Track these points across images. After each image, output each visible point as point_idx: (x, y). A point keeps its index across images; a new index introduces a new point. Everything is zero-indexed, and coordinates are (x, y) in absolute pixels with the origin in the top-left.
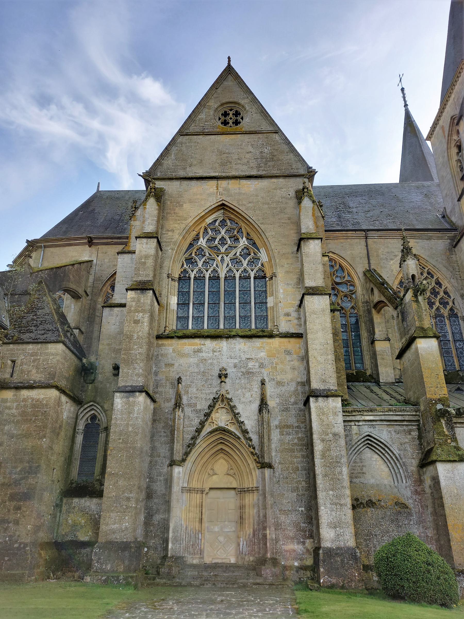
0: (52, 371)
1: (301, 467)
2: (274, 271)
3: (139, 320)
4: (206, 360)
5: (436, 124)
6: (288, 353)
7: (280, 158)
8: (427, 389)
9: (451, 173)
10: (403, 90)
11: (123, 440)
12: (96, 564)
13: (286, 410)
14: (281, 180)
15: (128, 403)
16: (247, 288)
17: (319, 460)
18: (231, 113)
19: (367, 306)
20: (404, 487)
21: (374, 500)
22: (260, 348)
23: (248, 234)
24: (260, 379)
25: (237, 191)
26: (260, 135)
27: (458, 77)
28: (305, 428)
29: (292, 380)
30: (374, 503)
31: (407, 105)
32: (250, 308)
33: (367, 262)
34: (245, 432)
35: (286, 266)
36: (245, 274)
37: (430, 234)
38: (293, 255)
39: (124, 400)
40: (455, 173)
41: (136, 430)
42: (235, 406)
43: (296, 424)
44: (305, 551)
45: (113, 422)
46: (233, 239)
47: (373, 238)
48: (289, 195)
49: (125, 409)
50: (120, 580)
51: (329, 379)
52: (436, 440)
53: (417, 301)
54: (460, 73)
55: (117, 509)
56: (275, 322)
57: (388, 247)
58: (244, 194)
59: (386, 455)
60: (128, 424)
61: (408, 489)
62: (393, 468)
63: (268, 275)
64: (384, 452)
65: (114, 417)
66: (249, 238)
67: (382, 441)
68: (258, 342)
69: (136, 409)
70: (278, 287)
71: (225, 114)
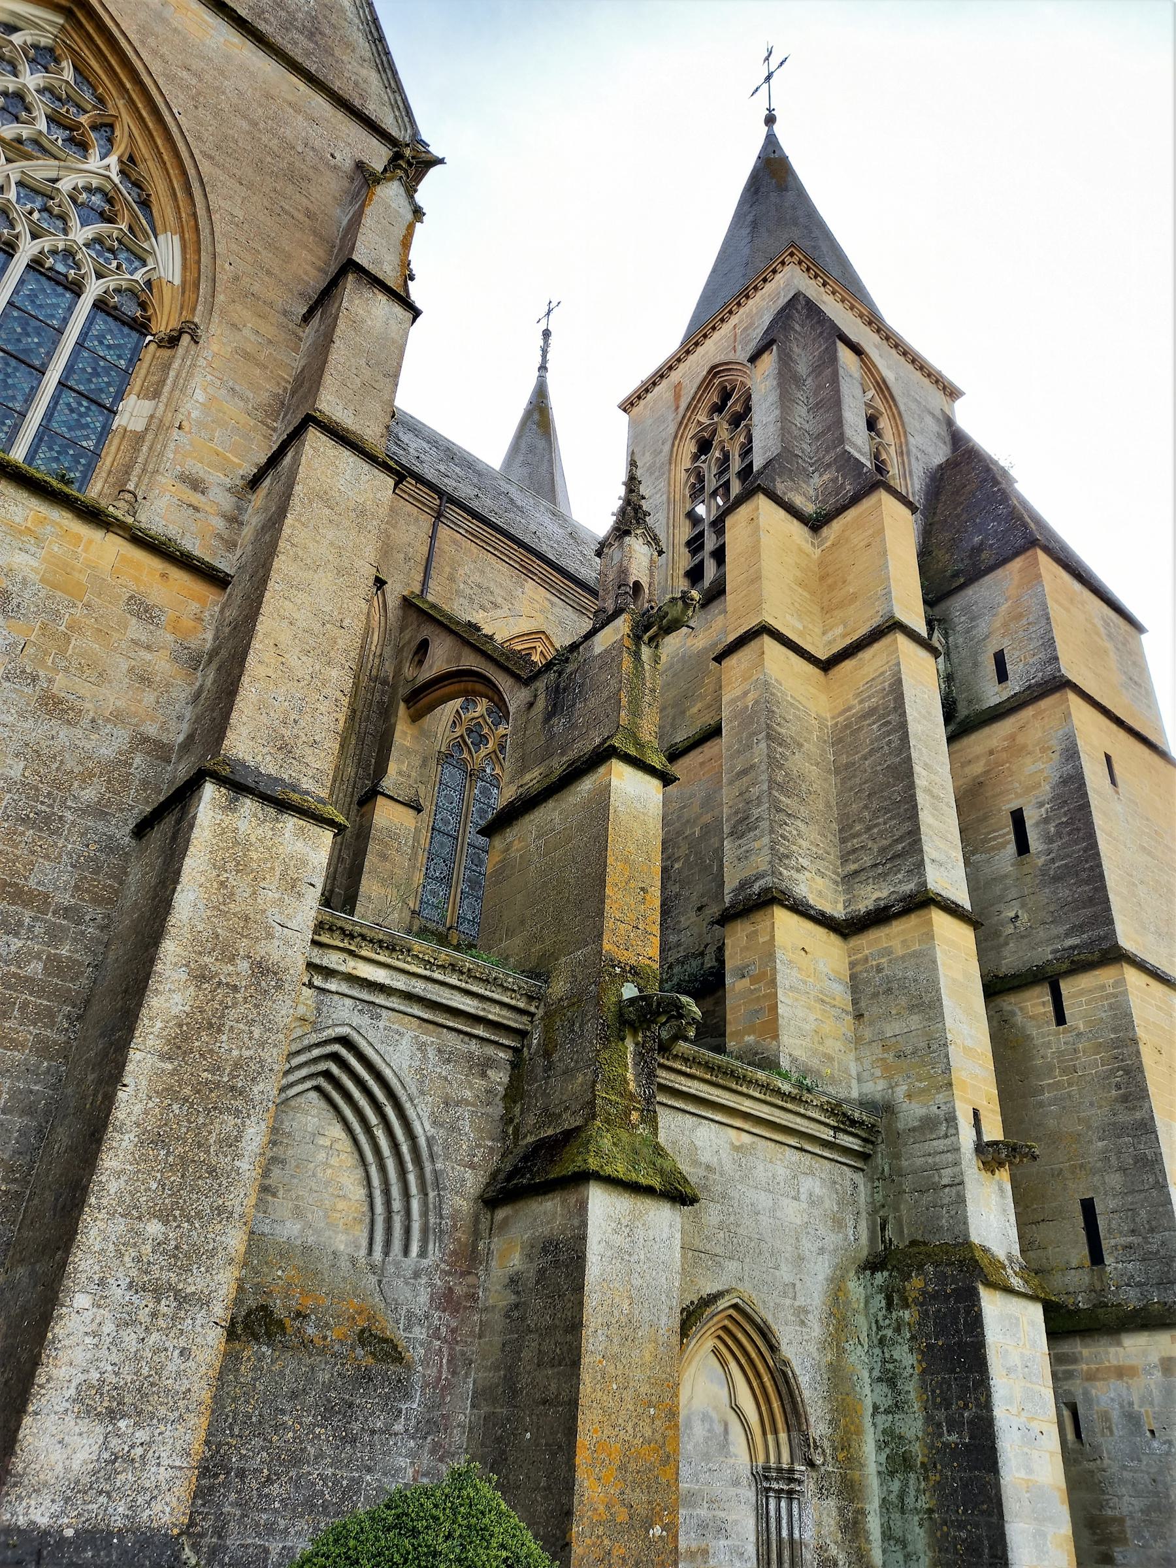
2: (196, 320)
5: (662, 376)
6: (143, 611)
7: (337, 53)
8: (609, 924)
9: (669, 492)
10: (547, 334)
13: (46, 823)
16: (52, 316)
17: (151, 1060)
19: (383, 693)
20: (409, 1273)
21: (280, 1312)
23: (131, 159)
27: (765, 280)
28: (102, 928)
29: (118, 717)
30: (280, 1324)
31: (546, 369)
32: (34, 390)
33: (420, 577)
35: (247, 332)
36: (60, 268)
38: (282, 319)
40: (677, 496)
43: (66, 899)
46: (59, 135)
47: (455, 527)
48: (332, 155)
51: (309, 751)
52: (598, 1101)
53: (637, 655)
54: (774, 272)
56: (134, 479)
57: (483, 572)
58: (175, 30)
59: (380, 1133)
61: (424, 1280)
62: (387, 1192)
63: (163, 323)
64: (373, 1119)
66: (129, 164)
67: (387, 1073)
70: (190, 375)
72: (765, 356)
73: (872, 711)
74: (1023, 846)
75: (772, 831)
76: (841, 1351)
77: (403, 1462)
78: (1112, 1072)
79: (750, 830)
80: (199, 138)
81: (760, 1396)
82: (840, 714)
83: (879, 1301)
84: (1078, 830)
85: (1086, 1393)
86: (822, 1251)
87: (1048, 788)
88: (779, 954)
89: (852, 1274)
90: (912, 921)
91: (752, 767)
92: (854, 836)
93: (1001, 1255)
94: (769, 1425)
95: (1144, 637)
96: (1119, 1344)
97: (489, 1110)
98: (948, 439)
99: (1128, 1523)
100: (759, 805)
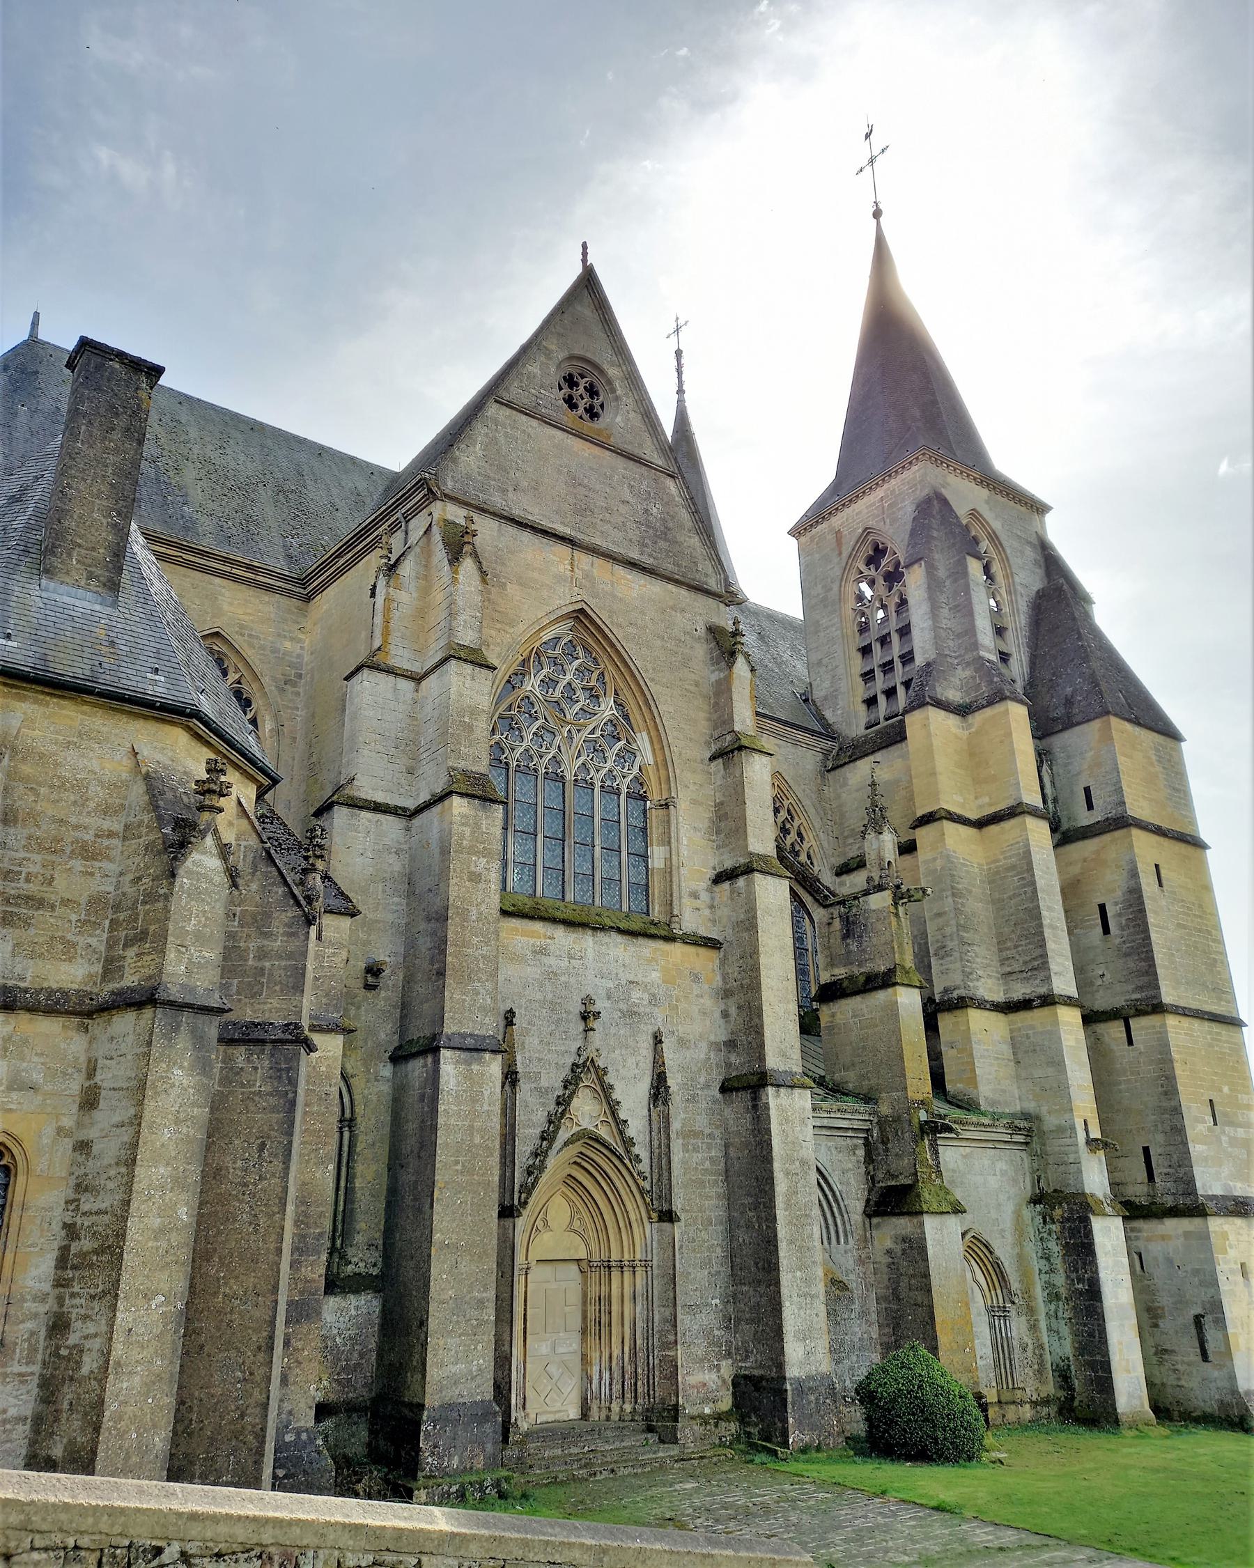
0: (334, 988)
1: (716, 1216)
3: (480, 875)
4: (556, 975)
11: (463, 1166)
12: (430, 1459)
14: (683, 593)
15: (468, 1076)
22: (651, 961)
24: (651, 1029)
25: (608, 588)
34: (628, 1143)
37: (800, 735)
39: (462, 1068)
41: (489, 1143)
42: (611, 1087)
43: (707, 1131)
44: (720, 1383)
49: (464, 1091)
50: (487, 1488)
53: (897, 915)
55: (460, 1328)
58: (621, 599)
60: (473, 1127)
68: (649, 948)
69: (486, 1093)
72: (916, 566)
73: (1013, 867)
74: (1106, 930)
75: (962, 960)
76: (1022, 1246)
77: (857, 1329)
78: (1159, 1077)
79: (947, 955)
80: (646, 671)
83: (1039, 1219)
84: (1139, 925)
85: (1146, 1247)
86: (1009, 1198)
87: (1120, 893)
88: (974, 1039)
89: (1024, 1207)
90: (1046, 1011)
91: (945, 913)
92: (1008, 949)
93: (1100, 1195)
96: (1163, 1224)
97: (859, 1171)
98: (1042, 563)
99: (1166, 1309)
100: (952, 940)
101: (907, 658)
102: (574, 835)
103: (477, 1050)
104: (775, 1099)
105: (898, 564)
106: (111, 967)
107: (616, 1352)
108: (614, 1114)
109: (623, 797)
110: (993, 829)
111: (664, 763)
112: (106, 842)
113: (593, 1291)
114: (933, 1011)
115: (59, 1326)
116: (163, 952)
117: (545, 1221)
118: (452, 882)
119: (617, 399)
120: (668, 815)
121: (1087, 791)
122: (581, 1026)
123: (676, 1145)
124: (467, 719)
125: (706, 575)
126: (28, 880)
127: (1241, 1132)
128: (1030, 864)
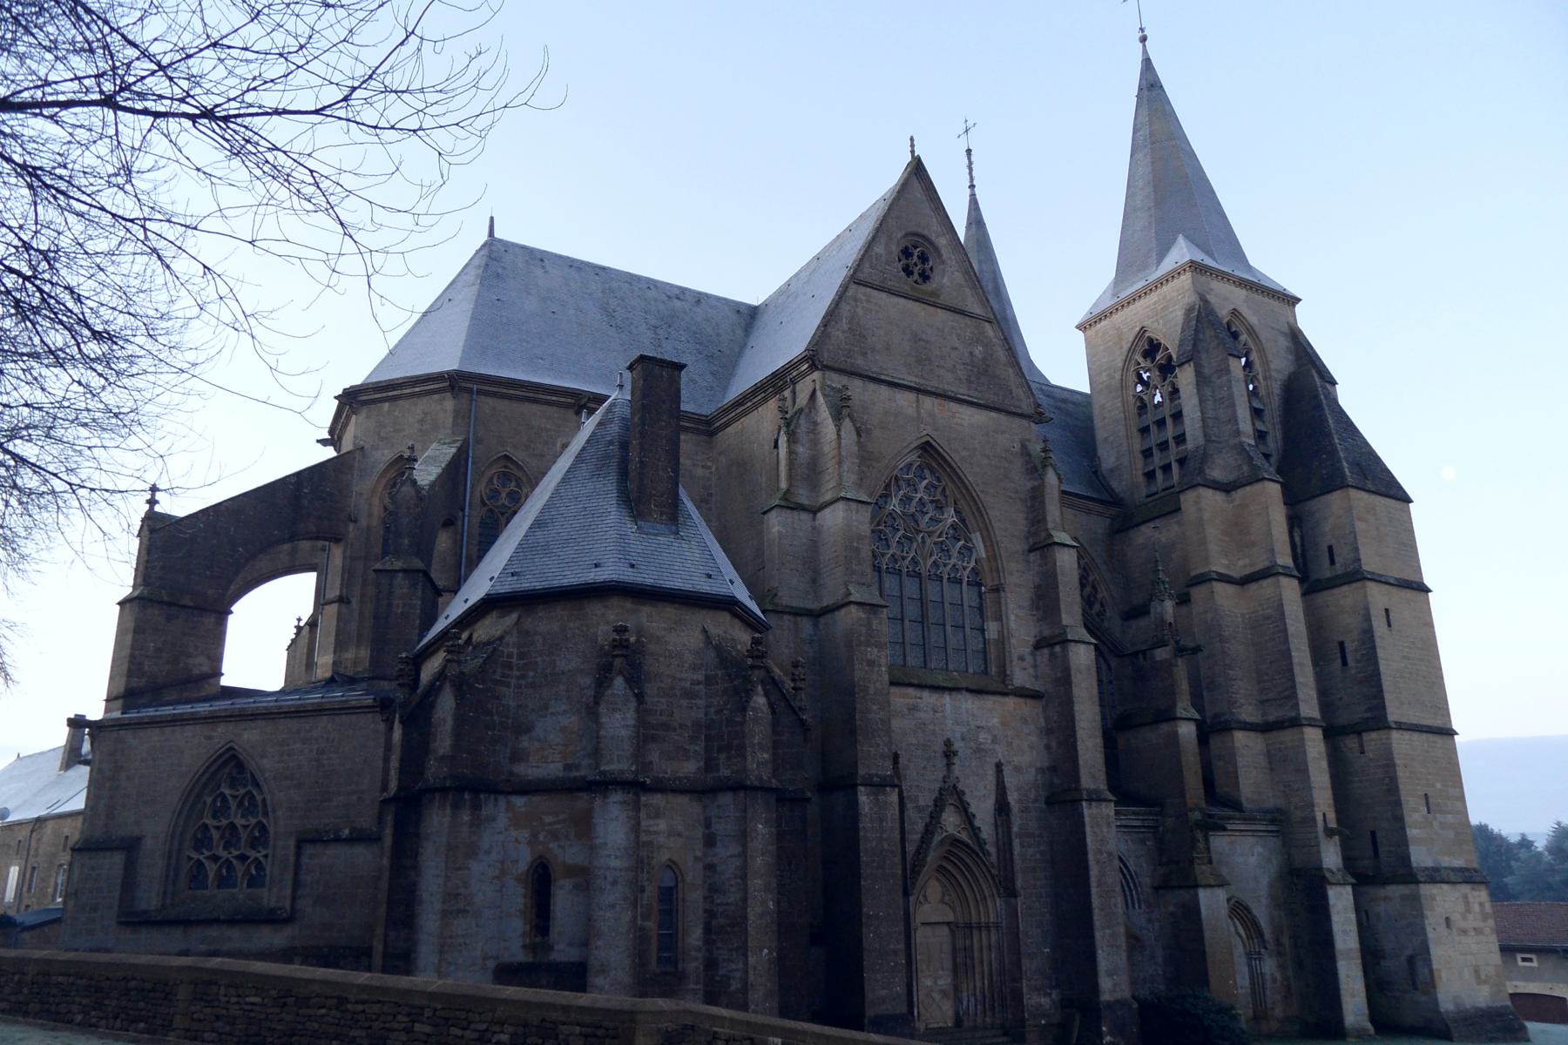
10: (969, 151)
14: (1002, 417)
18: (916, 252)
26: (967, 320)
34: (981, 843)
37: (1091, 505)
43: (1037, 832)
45: (862, 834)
65: (861, 826)
68: (990, 701)
71: (906, 253)
72: (1186, 366)
73: (1268, 618)
80: (978, 485)
81: (1246, 928)
82: (1253, 613)
94: (1249, 937)
95: (1411, 505)
101: (1180, 439)
102: (933, 616)
103: (881, 786)
104: (1089, 811)
105: (1170, 358)
106: (710, 765)
107: (978, 984)
108: (971, 823)
109: (965, 584)
110: (1253, 586)
111: (993, 557)
112: (697, 688)
113: (960, 944)
114: (1207, 731)
115: (711, 964)
116: (744, 757)
117: (925, 896)
118: (856, 667)
119: (943, 262)
120: (1000, 598)
121: (1330, 548)
122: (945, 761)
123: (1016, 843)
124: (855, 544)
125: (1019, 400)
126: (661, 715)
127: (1450, 818)
128: (1282, 615)
